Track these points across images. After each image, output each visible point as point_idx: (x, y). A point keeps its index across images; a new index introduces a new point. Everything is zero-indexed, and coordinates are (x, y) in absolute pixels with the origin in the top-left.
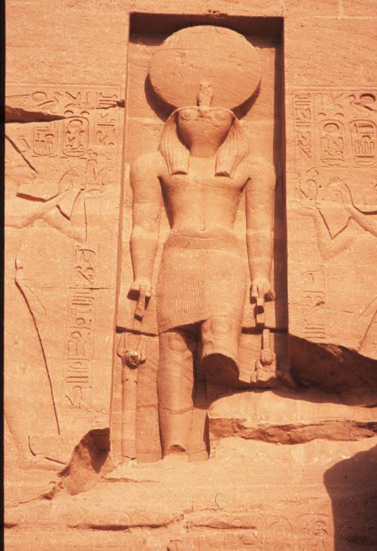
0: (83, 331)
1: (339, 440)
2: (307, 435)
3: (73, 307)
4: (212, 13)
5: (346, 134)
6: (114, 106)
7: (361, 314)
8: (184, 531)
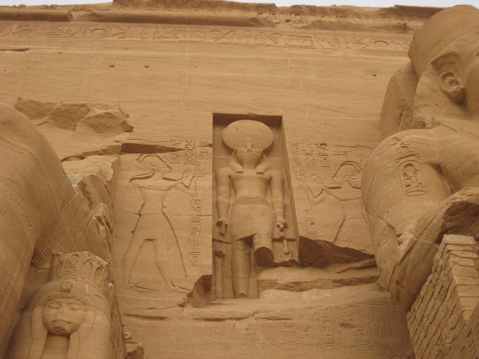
0: (197, 234)
1: (325, 289)
3: (192, 223)
4: (250, 114)
6: (207, 146)
7: (333, 228)
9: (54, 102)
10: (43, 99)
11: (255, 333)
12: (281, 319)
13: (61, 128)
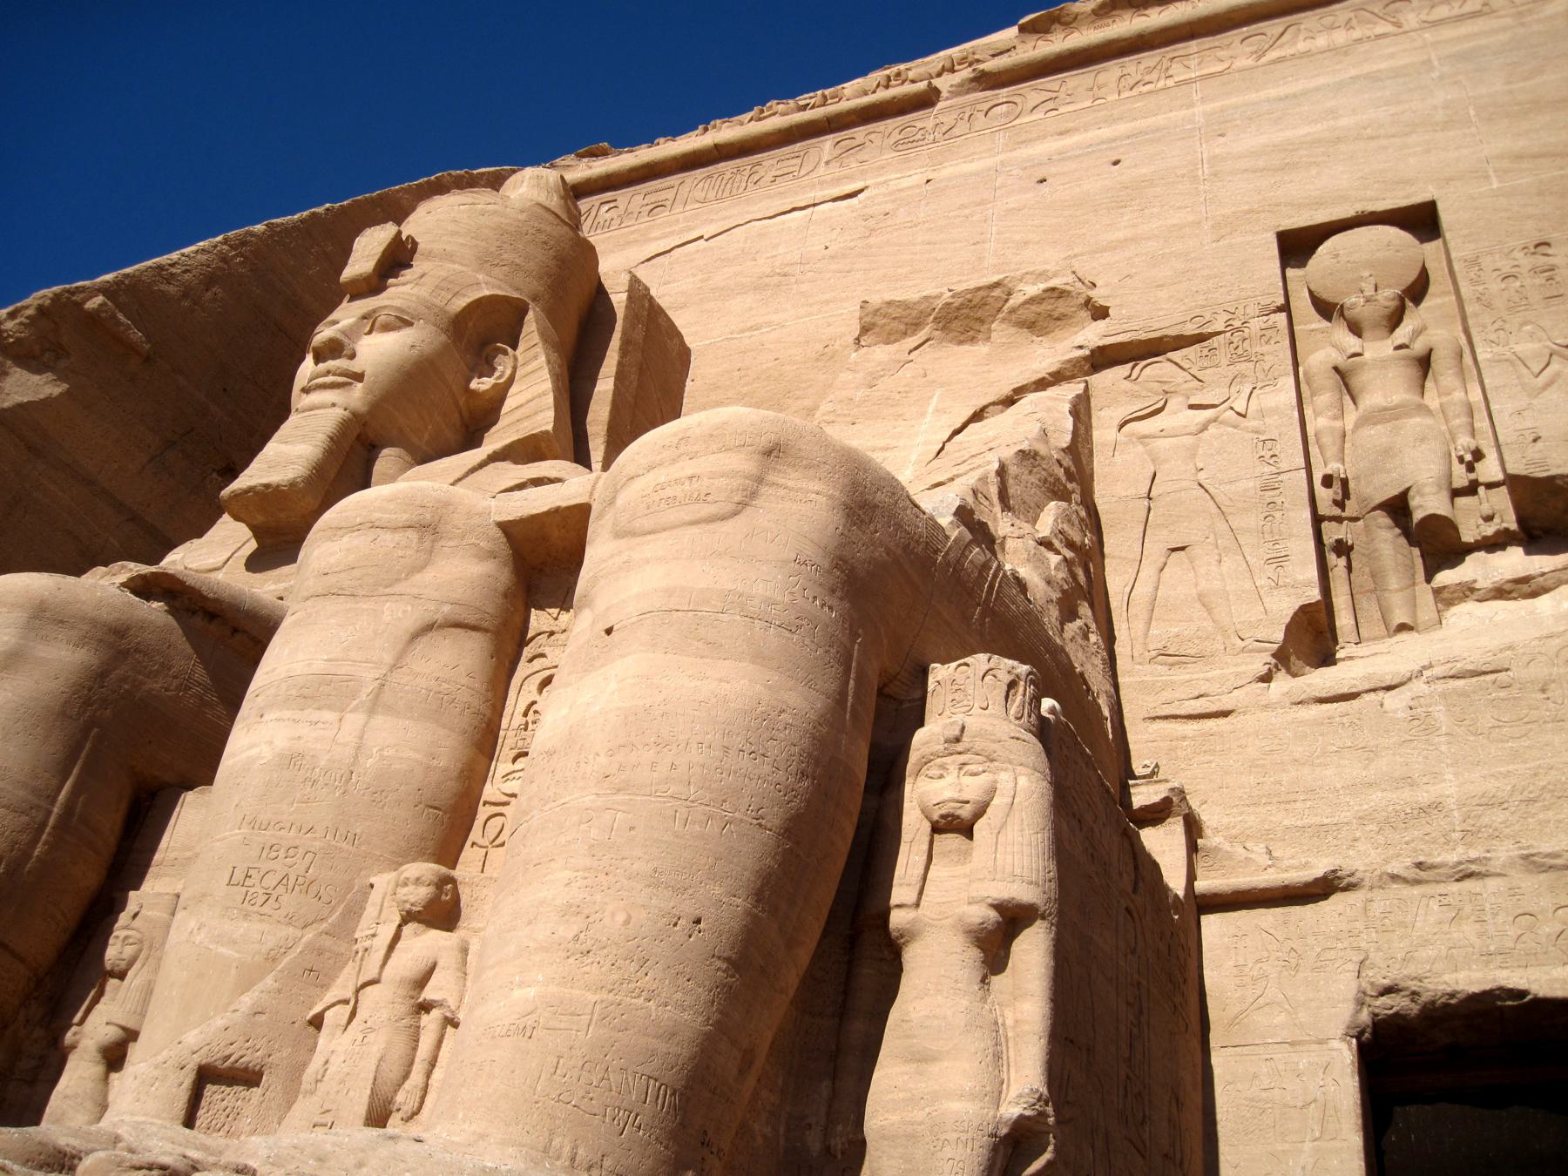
0: (1278, 515)
2: (1550, 583)
5: (1528, 282)
8: (1425, 687)
9: (935, 292)
10: (910, 293)
11: (1428, 714)
12: (1485, 673)
13: (961, 343)
